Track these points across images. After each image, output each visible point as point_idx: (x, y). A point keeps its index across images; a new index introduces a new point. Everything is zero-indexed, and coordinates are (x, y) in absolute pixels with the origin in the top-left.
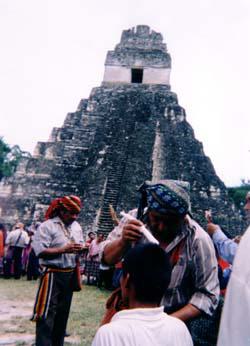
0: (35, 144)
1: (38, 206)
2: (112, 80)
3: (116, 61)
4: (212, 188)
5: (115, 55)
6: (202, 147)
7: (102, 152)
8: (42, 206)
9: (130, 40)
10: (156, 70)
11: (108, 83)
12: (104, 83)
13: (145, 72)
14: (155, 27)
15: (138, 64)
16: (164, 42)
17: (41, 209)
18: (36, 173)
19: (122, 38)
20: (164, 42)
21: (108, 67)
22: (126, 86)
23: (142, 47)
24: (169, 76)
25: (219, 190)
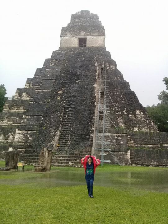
0: (15, 90)
1: (17, 132)
2: (63, 46)
4: (138, 112)
5: (65, 31)
6: (129, 85)
7: (60, 92)
8: (20, 132)
9: (77, 20)
10: (95, 38)
12: (60, 48)
13: (88, 38)
14: (93, 11)
15: (83, 34)
16: (99, 20)
17: (19, 133)
18: (17, 110)
20: (99, 20)
22: (75, 48)
23: (84, 25)
24: (104, 41)
25: (142, 113)
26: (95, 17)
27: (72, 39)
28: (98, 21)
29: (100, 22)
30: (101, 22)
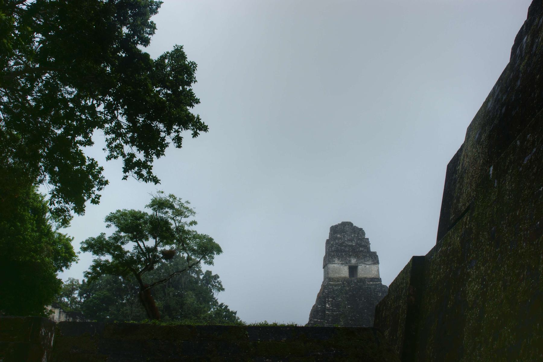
3: (336, 261)
9: (339, 236)
10: (368, 266)
11: (333, 279)
13: (360, 267)
14: (357, 224)
15: (353, 261)
19: (331, 234)
21: (331, 266)
24: (378, 271)
26: (360, 232)
27: (342, 267)
28: (364, 238)
29: (368, 239)
30: (368, 239)
